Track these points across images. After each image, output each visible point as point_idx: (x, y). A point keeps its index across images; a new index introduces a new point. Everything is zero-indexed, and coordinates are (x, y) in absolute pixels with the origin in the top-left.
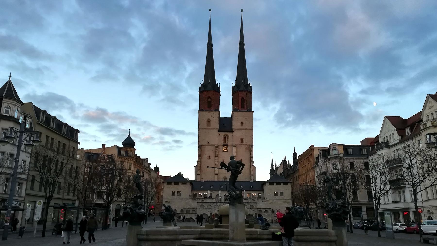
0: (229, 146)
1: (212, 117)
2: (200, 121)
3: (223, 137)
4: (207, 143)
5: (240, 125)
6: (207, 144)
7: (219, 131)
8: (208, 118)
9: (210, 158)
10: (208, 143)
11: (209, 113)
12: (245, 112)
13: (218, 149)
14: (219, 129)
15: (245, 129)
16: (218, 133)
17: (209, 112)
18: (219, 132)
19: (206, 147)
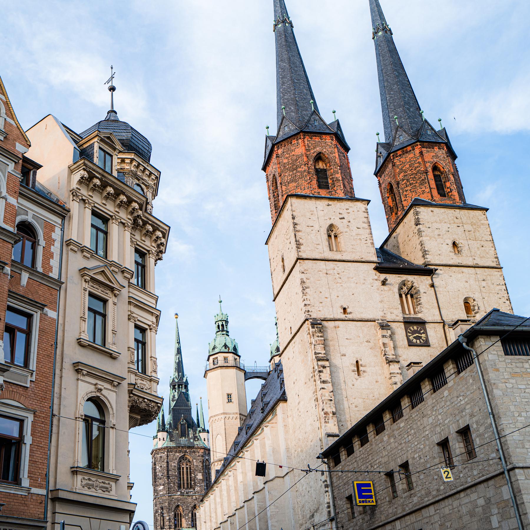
0: (427, 326)
1: (344, 218)
2: (299, 231)
3: (396, 290)
4: (342, 311)
5: (451, 252)
6: (343, 316)
7: (380, 269)
8: (329, 223)
9: (361, 368)
10: (345, 309)
11: (328, 205)
12: (458, 211)
13: (390, 336)
14: (378, 263)
15: (475, 267)
16: (376, 277)
17: (330, 203)
18: (378, 274)
19: (338, 327)
